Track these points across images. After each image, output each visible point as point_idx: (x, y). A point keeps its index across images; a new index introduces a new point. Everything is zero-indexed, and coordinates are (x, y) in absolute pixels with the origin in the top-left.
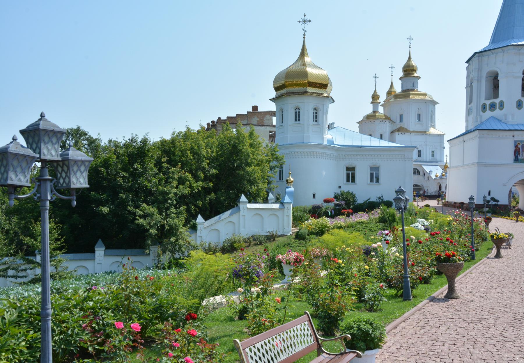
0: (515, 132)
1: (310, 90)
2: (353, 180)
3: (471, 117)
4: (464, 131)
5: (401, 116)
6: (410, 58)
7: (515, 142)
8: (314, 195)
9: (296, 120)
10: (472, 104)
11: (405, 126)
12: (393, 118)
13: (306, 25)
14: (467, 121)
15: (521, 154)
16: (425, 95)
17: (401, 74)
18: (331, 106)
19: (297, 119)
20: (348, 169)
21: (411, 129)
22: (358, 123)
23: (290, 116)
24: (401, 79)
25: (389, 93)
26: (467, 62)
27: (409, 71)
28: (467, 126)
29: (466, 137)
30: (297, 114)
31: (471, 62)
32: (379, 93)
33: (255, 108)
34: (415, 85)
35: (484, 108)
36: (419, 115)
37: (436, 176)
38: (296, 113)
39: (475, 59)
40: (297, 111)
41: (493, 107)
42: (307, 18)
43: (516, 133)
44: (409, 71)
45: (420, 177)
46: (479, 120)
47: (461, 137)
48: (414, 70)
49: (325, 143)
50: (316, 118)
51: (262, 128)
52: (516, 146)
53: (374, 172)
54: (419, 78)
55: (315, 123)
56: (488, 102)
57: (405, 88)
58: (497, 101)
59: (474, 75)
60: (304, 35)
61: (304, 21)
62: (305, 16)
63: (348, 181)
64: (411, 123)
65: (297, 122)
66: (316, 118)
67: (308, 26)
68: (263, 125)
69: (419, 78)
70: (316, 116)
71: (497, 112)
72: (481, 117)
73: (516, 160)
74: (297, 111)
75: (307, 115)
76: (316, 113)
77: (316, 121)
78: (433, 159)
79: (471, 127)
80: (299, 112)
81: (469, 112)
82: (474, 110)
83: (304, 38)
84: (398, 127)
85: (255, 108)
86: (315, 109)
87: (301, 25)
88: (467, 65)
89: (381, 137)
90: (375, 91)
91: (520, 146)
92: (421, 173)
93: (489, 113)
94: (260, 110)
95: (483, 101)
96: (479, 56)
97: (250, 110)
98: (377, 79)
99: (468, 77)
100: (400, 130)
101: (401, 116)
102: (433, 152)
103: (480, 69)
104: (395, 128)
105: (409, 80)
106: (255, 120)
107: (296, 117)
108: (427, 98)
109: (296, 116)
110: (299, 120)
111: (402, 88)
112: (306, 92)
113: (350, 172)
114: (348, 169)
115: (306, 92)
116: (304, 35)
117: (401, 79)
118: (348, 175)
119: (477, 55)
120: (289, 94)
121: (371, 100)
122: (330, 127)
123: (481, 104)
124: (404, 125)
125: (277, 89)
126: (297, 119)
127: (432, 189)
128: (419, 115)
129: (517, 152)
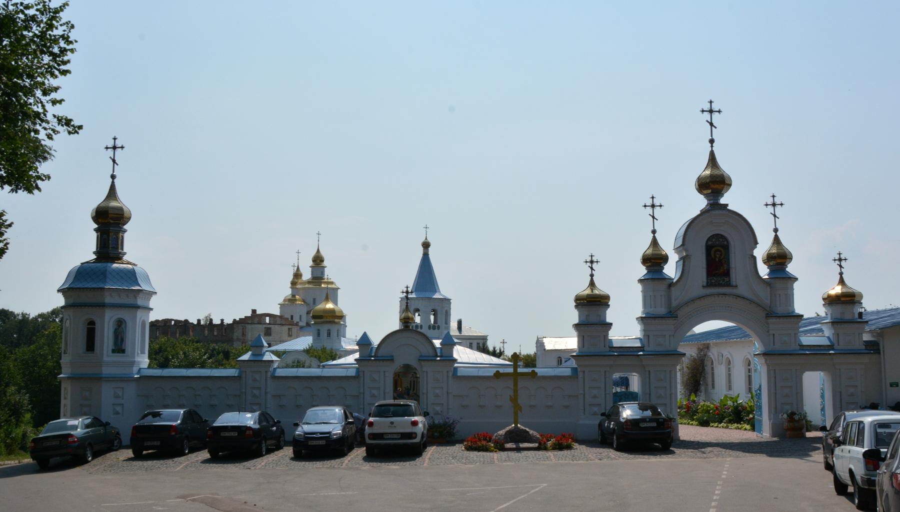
5: (314, 300)
6: (318, 250)
16: (332, 283)
17: (311, 263)
23: (324, 333)
27: (318, 260)
33: (254, 311)
34: (323, 273)
44: (318, 260)
48: (322, 261)
51: (260, 326)
68: (260, 324)
85: (254, 311)
94: (258, 312)
101: (314, 300)
106: (256, 320)
108: (333, 286)
112: (334, 322)
115: (334, 322)
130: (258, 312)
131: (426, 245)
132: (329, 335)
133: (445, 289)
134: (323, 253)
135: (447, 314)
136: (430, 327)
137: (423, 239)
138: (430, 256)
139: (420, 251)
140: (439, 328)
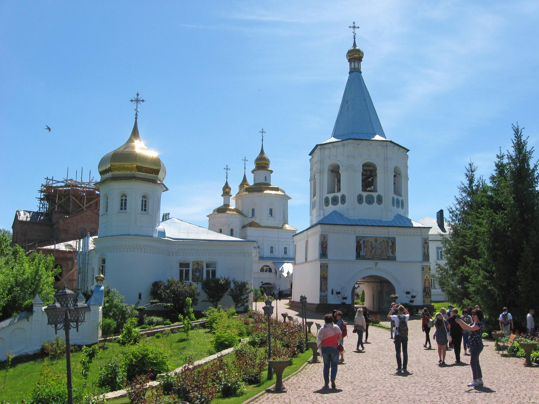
3: (315, 210)
4: (309, 226)
5: (253, 210)
6: (262, 152)
7: (357, 237)
8: (140, 295)
9: (121, 209)
10: (315, 198)
11: (257, 221)
12: (245, 212)
13: (139, 105)
14: (311, 214)
15: (362, 250)
16: (277, 189)
17: (253, 167)
18: (164, 194)
19: (123, 207)
21: (263, 225)
24: (253, 172)
25: (242, 185)
26: (311, 154)
27: (262, 164)
28: (311, 221)
29: (309, 232)
30: (124, 202)
31: (314, 154)
32: (230, 185)
36: (271, 210)
37: (288, 273)
38: (122, 200)
39: (317, 151)
40: (124, 198)
41: (335, 201)
42: (141, 97)
43: (358, 228)
44: (262, 164)
45: (272, 275)
46: (322, 214)
47: (305, 232)
49: (156, 235)
50: (145, 207)
52: (358, 242)
53: (211, 269)
54: (272, 172)
55: (144, 212)
56: (330, 196)
57: (258, 182)
58: (339, 195)
59: (316, 166)
60: (136, 115)
61: (137, 101)
62: (138, 95)
64: (262, 218)
65: (123, 211)
66: (144, 206)
67: (141, 105)
69: (272, 172)
70: (145, 205)
71: (339, 207)
72: (324, 210)
73: (358, 256)
74: (124, 198)
75: (134, 203)
76: (145, 201)
77: (145, 210)
78: (286, 256)
79: (315, 222)
80: (126, 200)
81: (313, 205)
82: (317, 204)
83: (136, 118)
84: (250, 220)
86: (144, 197)
87: (134, 105)
88: (311, 157)
89: (221, 232)
90: (227, 183)
91: (361, 242)
92: (273, 271)
93: (331, 208)
95: (325, 195)
96: (321, 149)
98: (228, 171)
100: (252, 224)
101: (253, 210)
102: (285, 248)
103: (322, 161)
104: (246, 223)
105: (262, 173)
107: (122, 205)
109: (122, 203)
110: (125, 209)
111: (254, 181)
113: (184, 269)
114: (181, 265)
116: (136, 115)
117: (253, 172)
118: (181, 272)
119: (319, 147)
120: (114, 178)
121: (222, 193)
122: (166, 217)
123: (324, 197)
124: (256, 220)
125: (102, 173)
126: (123, 207)
127: (284, 287)
128: (271, 210)
129: (358, 248)
131: (355, 56)
132: (123, 205)
133: (392, 119)
134: (267, 154)
135: (399, 177)
136: (360, 199)
137: (351, 47)
138: (365, 74)
139: (346, 66)
140: (380, 200)
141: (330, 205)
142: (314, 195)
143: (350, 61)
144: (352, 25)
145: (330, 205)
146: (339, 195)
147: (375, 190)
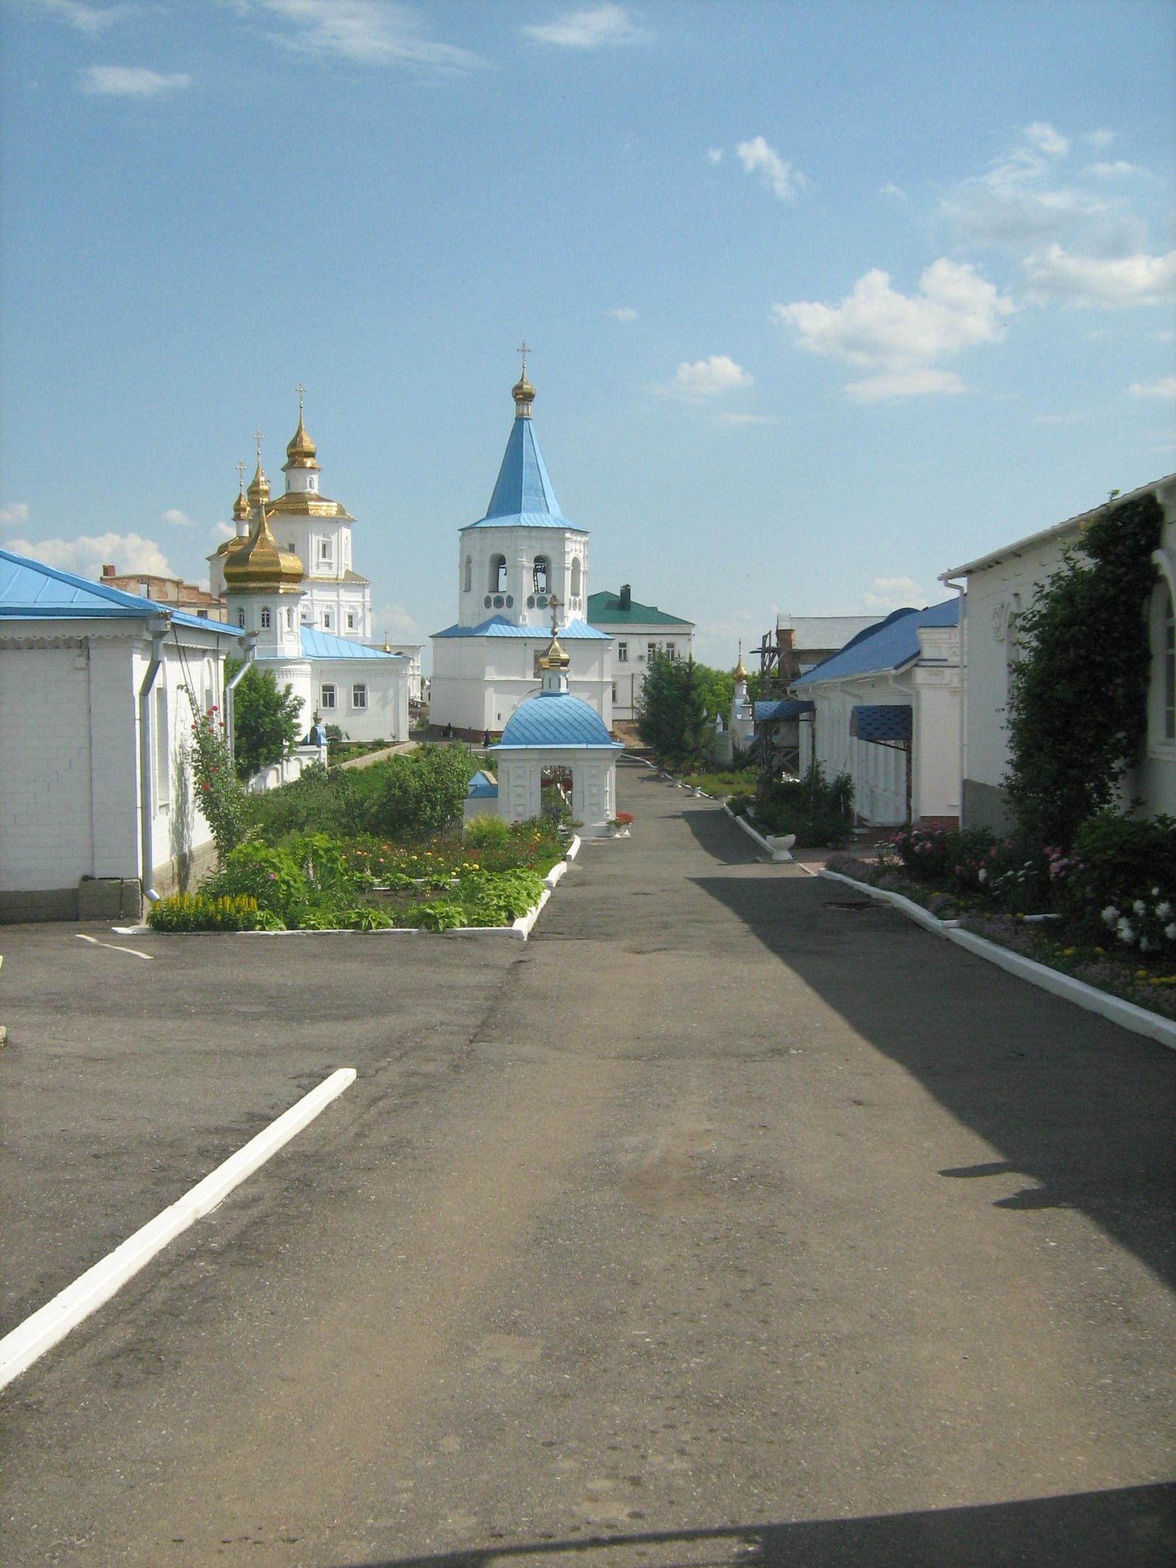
0: (528, 641)
1: (283, 587)
2: (332, 705)
17: (285, 460)
20: (325, 688)
22: (208, 559)
25: (254, 491)
31: (466, 532)
35: (487, 603)
41: (499, 602)
56: (493, 596)
57: (294, 490)
63: (325, 705)
71: (504, 611)
93: (494, 611)
94: (118, 574)
95: (486, 593)
97: (102, 574)
99: (462, 552)
111: (288, 486)
114: (325, 688)
118: (325, 696)
125: (229, 577)
128: (324, 546)
130: (118, 574)
131: (523, 396)
139: (510, 408)
141: (493, 607)
142: (468, 589)
143: (517, 400)
144: (521, 347)
145: (493, 607)
146: (505, 596)
147: (549, 592)
